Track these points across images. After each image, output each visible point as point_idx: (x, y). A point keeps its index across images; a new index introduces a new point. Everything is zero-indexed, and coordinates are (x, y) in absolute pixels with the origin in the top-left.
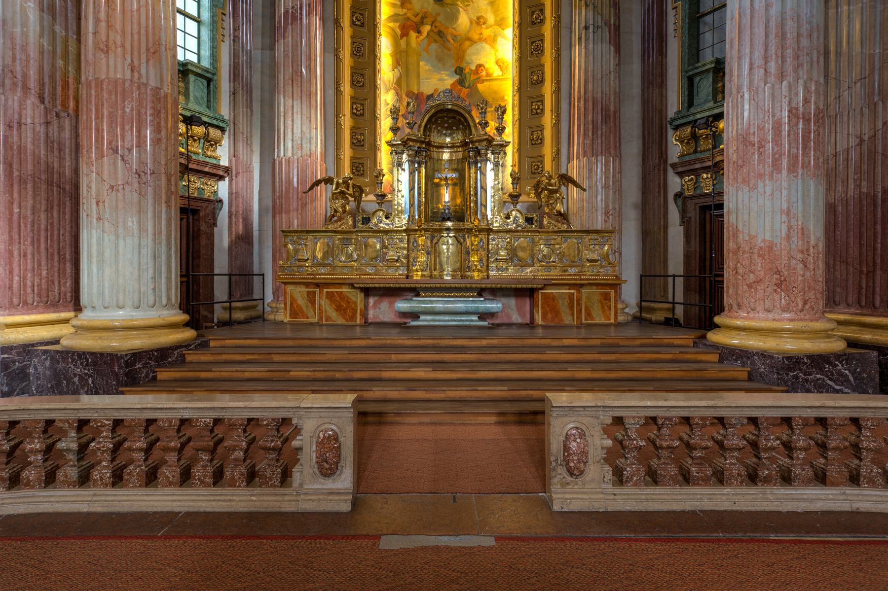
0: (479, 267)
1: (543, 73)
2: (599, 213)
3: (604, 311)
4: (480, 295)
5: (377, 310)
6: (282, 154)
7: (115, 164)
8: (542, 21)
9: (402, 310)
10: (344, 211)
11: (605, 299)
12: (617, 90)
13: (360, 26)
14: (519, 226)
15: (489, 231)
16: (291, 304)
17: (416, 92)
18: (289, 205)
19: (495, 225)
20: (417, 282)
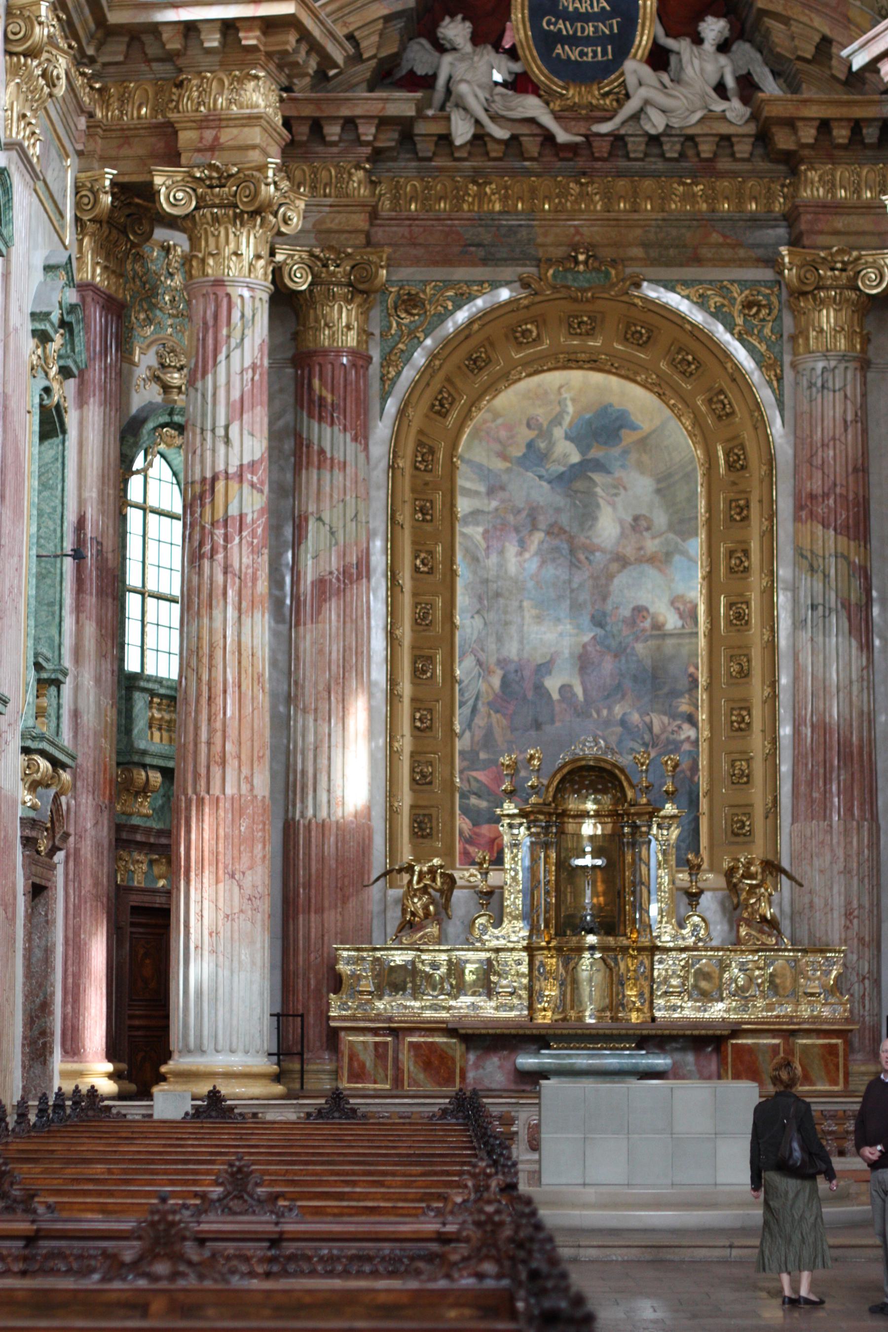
0: (638, 1004)
1: (749, 661)
2: (836, 914)
3: (828, 1072)
4: (639, 1047)
5: (481, 1071)
6: (310, 812)
7: (231, 890)
8: (746, 570)
9: (527, 1068)
10: (427, 915)
11: (830, 1054)
12: (865, 709)
13: (428, 573)
14: (700, 940)
15: (654, 949)
16: (351, 1059)
17: (516, 658)
18: (322, 900)
19: (663, 939)
20: (548, 1027)
